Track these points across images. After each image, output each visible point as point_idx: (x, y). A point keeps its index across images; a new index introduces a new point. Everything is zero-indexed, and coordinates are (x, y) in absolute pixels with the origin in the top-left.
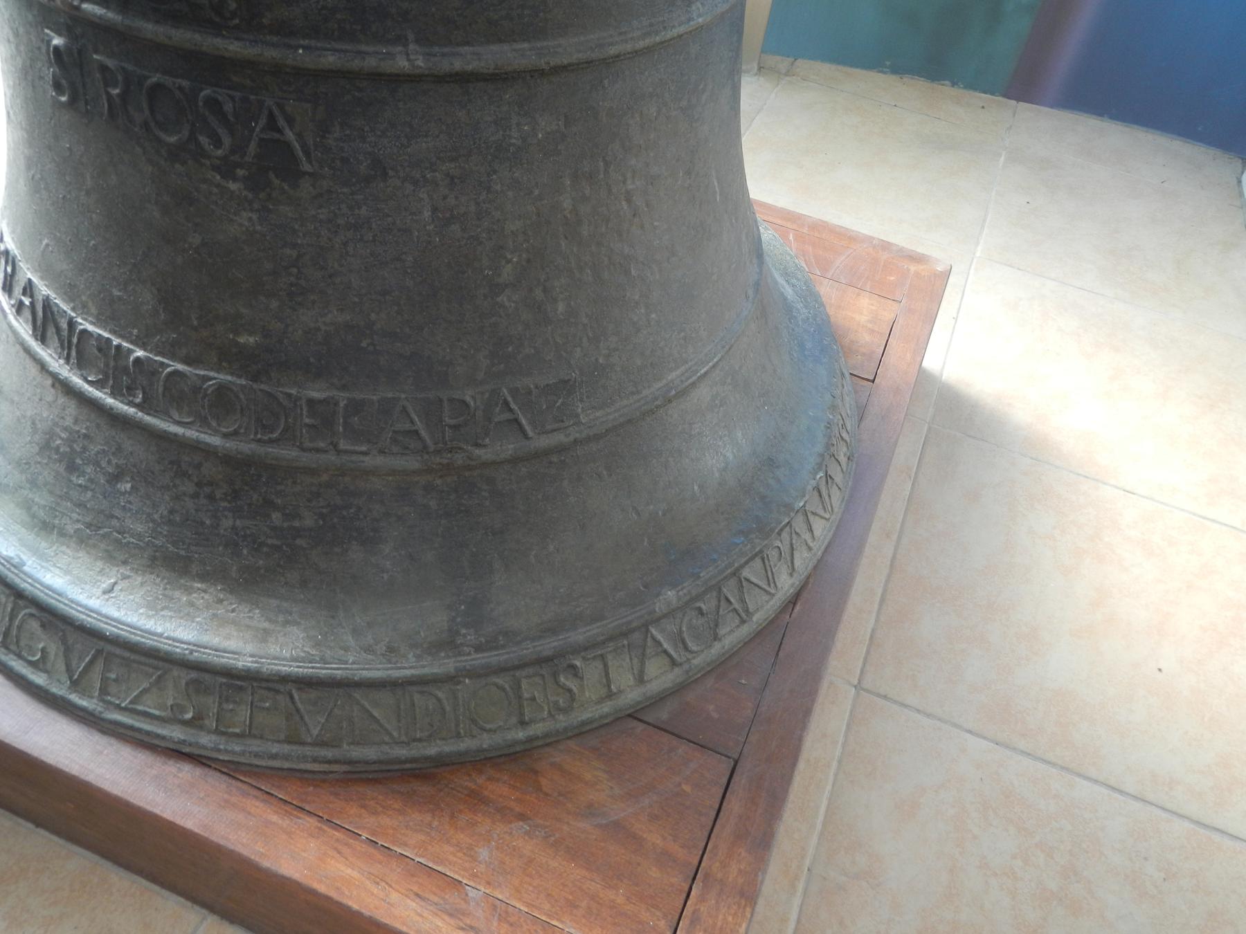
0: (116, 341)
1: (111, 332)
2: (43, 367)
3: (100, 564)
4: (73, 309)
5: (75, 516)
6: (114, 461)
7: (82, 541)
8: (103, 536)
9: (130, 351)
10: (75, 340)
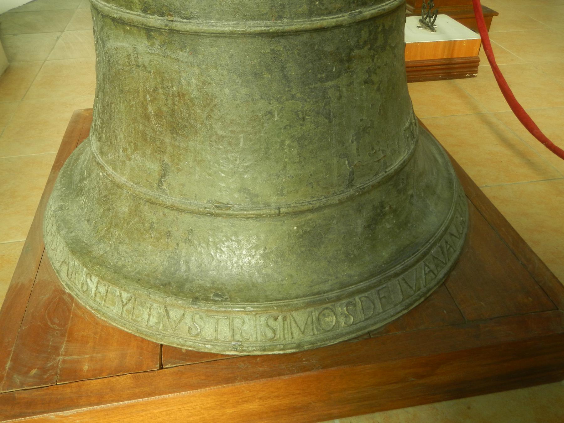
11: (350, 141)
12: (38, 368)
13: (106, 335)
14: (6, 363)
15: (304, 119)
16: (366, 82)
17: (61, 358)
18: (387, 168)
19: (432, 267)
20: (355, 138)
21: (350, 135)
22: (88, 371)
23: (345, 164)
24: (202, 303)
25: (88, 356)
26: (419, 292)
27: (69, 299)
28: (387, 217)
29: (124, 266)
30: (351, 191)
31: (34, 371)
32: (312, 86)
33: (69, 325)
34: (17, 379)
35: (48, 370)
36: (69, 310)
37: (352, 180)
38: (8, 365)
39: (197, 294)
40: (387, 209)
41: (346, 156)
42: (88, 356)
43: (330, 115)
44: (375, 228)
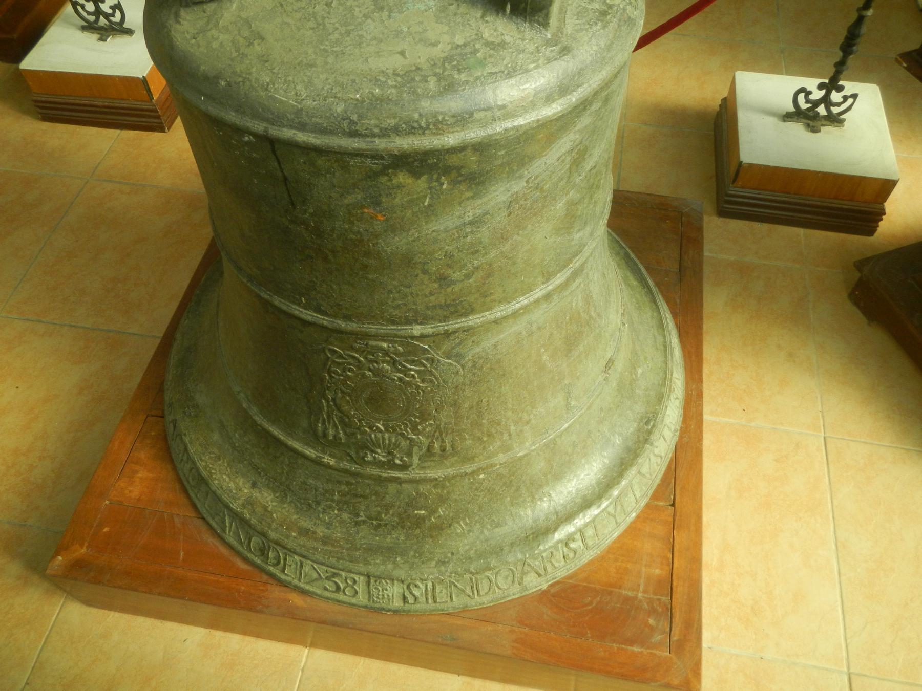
12: (649, 617)
13: (622, 549)
14: (633, 652)
17: (640, 595)
22: (662, 569)
24: (653, 437)
27: (557, 587)
31: (651, 621)
33: (598, 587)
34: (657, 638)
36: (575, 586)
39: (641, 438)
42: (644, 569)
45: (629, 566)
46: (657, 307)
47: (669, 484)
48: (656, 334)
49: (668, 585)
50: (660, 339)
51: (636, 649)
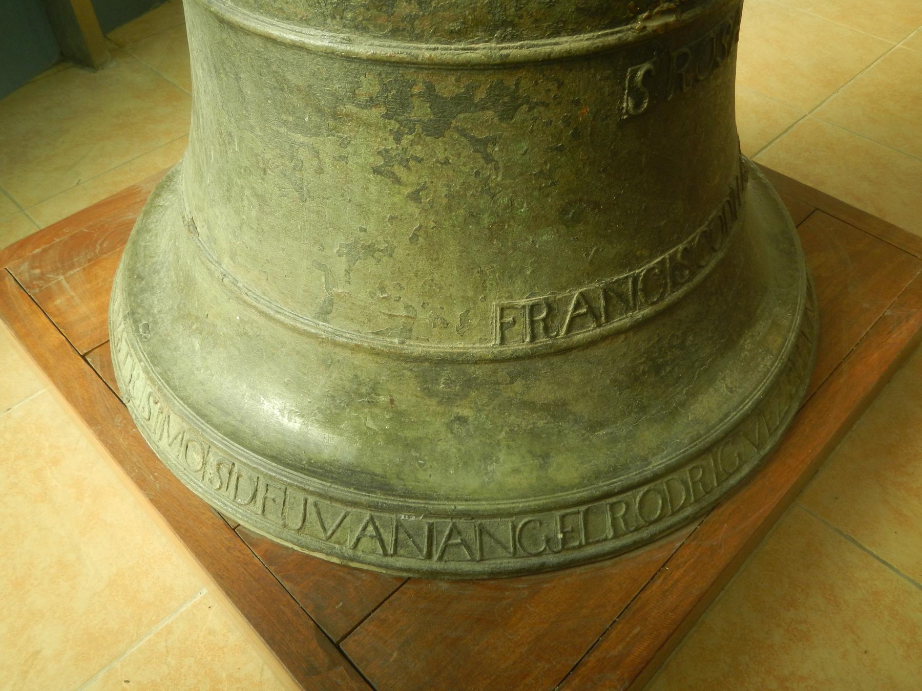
0: (667, 255)
1: (661, 255)
2: (618, 332)
3: (711, 390)
4: (630, 271)
5: (678, 390)
6: (679, 333)
7: (693, 395)
8: (699, 377)
9: (676, 253)
10: (640, 285)
11: (335, 251)
15: (265, 171)
16: (376, 171)
17: (61, 277)
18: (410, 338)
19: (389, 538)
20: (346, 251)
21: (337, 242)
23: (320, 280)
24: (129, 321)
25: (73, 294)
26: (337, 546)
28: (377, 411)
29: (149, 231)
30: (323, 328)
31: (37, 271)
32: (274, 128)
35: (42, 279)
37: (328, 313)
38: (38, 251)
39: (140, 310)
40: (382, 398)
41: (321, 266)
42: (73, 294)
43: (301, 188)
44: (344, 408)
45: (88, 286)
46: (264, 455)
47: (102, 367)
48: (229, 419)
49: (40, 303)
50: (218, 418)
51: (38, 251)
